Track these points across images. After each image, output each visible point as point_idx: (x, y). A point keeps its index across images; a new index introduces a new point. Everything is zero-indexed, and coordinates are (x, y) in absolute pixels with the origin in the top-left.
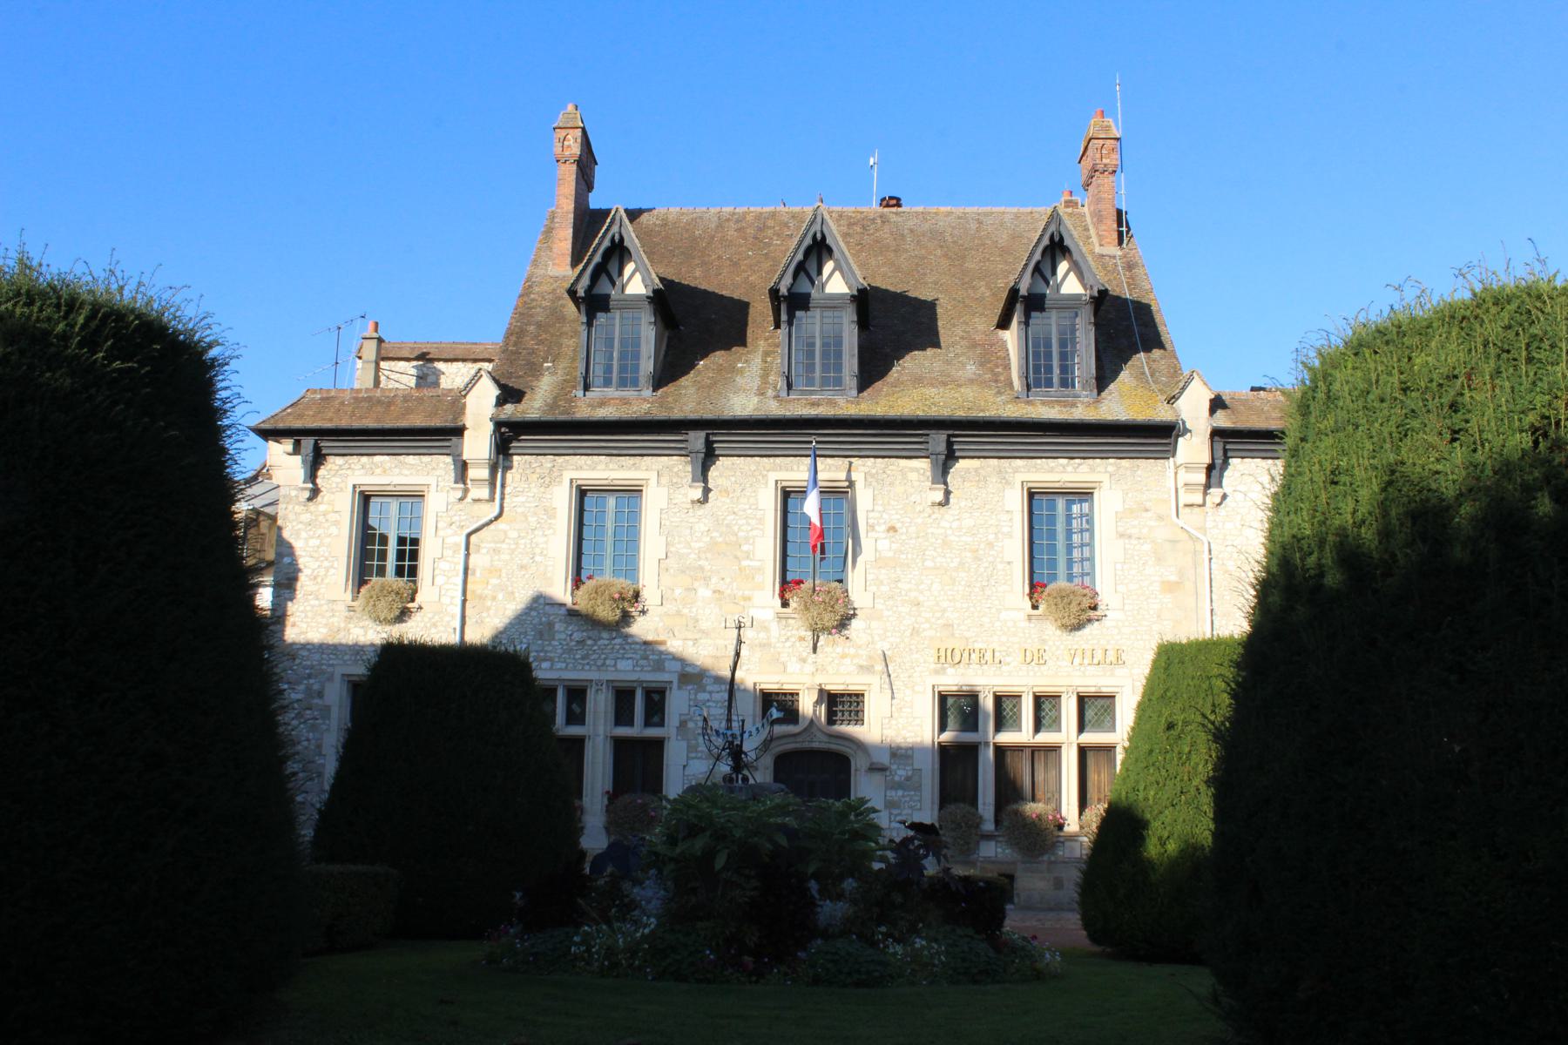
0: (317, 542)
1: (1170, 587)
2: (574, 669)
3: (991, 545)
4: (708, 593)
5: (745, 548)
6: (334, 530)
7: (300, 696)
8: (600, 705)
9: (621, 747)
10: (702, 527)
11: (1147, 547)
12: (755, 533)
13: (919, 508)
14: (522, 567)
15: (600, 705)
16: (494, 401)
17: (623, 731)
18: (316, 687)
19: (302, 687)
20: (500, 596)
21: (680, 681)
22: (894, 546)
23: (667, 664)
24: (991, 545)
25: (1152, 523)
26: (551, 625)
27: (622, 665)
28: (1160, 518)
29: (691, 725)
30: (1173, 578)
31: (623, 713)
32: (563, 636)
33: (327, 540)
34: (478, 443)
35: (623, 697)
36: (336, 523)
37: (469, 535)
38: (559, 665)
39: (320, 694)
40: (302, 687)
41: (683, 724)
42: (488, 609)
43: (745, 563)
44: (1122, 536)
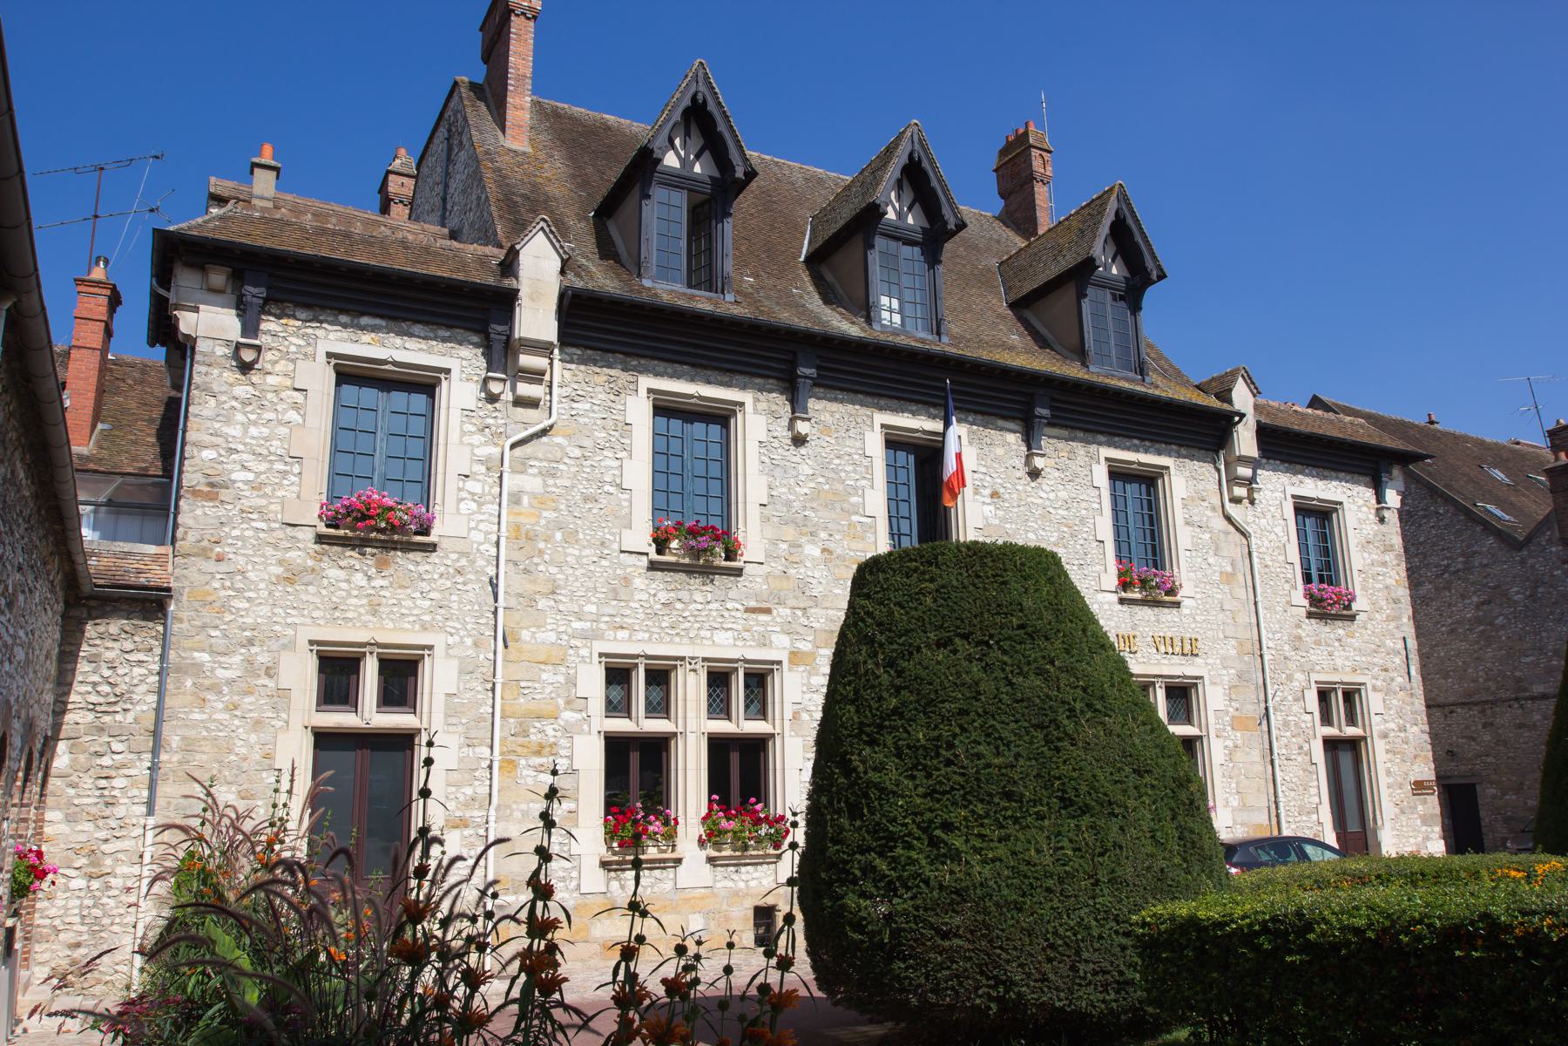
0: (266, 431)
1: (1228, 578)
2: (660, 641)
3: (1083, 521)
4: (816, 552)
5: (854, 499)
6: (293, 416)
7: (229, 674)
8: (691, 689)
9: (719, 747)
10: (806, 469)
11: (1207, 536)
12: (864, 483)
13: (1019, 474)
14: (586, 499)
15: (691, 689)
16: (558, 264)
17: (722, 727)
18: (263, 658)
19: (237, 659)
20: (559, 536)
21: (791, 662)
22: (1000, 513)
23: (774, 637)
24: (1083, 521)
25: (1209, 513)
26: (627, 581)
27: (721, 637)
28: (1214, 509)
29: (805, 716)
30: (1229, 569)
31: (719, 704)
32: (645, 596)
33: (284, 431)
34: (536, 318)
35: (719, 680)
36: (296, 407)
37: (513, 446)
38: (640, 635)
39: (269, 672)
40: (237, 659)
41: (796, 716)
42: (541, 552)
43: (855, 518)
44: (1187, 523)
